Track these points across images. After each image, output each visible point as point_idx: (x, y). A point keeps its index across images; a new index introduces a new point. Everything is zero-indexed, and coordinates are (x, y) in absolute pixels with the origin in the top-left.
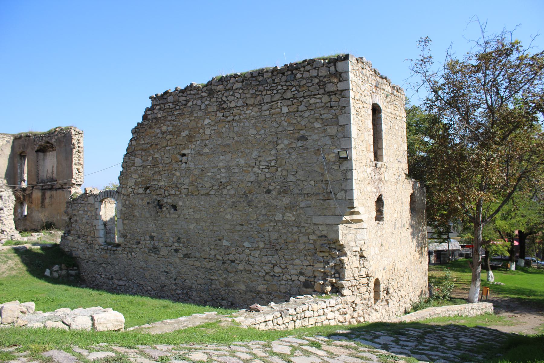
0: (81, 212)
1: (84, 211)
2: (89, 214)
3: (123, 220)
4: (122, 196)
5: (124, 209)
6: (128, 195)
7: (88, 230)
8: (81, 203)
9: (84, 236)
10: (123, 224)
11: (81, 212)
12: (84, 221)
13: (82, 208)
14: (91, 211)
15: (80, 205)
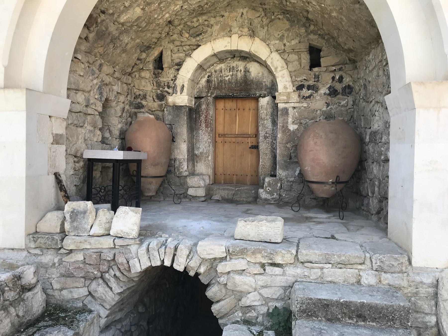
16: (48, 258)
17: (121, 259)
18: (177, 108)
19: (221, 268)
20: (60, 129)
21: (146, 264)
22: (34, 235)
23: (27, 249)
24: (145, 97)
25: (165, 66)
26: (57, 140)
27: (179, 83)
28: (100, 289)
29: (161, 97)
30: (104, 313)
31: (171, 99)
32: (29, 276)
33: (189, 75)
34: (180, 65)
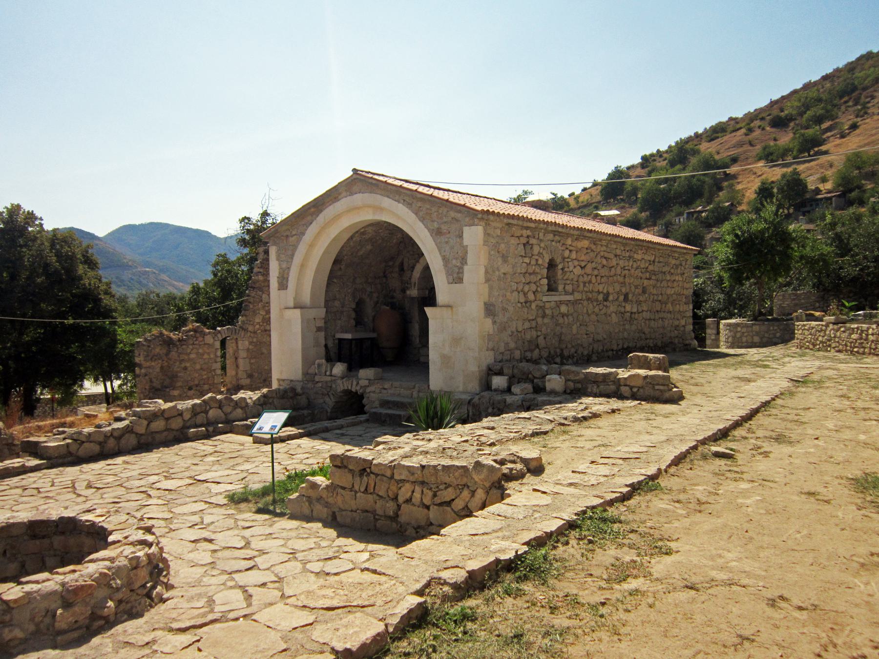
0: (193, 356)
1: (197, 353)
2: (206, 356)
3: (250, 359)
4: (249, 334)
5: (251, 347)
6: (255, 332)
7: (205, 377)
8: (193, 344)
9: (197, 386)
10: (251, 364)
11: (193, 356)
12: (198, 367)
13: (195, 351)
14: (209, 354)
15: (191, 347)
16: (310, 385)
17: (334, 386)
18: (413, 299)
19: (368, 390)
20: (321, 324)
21: (342, 388)
22: (305, 374)
23: (303, 381)
24: (395, 291)
25: (405, 268)
26: (319, 329)
27: (413, 280)
28: (327, 399)
29: (404, 291)
30: (329, 410)
31: (408, 292)
32: (299, 390)
33: (418, 275)
34: (413, 267)
